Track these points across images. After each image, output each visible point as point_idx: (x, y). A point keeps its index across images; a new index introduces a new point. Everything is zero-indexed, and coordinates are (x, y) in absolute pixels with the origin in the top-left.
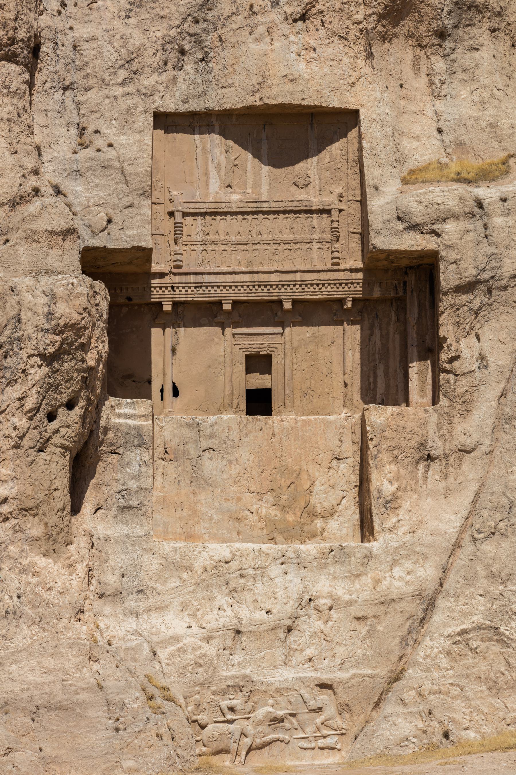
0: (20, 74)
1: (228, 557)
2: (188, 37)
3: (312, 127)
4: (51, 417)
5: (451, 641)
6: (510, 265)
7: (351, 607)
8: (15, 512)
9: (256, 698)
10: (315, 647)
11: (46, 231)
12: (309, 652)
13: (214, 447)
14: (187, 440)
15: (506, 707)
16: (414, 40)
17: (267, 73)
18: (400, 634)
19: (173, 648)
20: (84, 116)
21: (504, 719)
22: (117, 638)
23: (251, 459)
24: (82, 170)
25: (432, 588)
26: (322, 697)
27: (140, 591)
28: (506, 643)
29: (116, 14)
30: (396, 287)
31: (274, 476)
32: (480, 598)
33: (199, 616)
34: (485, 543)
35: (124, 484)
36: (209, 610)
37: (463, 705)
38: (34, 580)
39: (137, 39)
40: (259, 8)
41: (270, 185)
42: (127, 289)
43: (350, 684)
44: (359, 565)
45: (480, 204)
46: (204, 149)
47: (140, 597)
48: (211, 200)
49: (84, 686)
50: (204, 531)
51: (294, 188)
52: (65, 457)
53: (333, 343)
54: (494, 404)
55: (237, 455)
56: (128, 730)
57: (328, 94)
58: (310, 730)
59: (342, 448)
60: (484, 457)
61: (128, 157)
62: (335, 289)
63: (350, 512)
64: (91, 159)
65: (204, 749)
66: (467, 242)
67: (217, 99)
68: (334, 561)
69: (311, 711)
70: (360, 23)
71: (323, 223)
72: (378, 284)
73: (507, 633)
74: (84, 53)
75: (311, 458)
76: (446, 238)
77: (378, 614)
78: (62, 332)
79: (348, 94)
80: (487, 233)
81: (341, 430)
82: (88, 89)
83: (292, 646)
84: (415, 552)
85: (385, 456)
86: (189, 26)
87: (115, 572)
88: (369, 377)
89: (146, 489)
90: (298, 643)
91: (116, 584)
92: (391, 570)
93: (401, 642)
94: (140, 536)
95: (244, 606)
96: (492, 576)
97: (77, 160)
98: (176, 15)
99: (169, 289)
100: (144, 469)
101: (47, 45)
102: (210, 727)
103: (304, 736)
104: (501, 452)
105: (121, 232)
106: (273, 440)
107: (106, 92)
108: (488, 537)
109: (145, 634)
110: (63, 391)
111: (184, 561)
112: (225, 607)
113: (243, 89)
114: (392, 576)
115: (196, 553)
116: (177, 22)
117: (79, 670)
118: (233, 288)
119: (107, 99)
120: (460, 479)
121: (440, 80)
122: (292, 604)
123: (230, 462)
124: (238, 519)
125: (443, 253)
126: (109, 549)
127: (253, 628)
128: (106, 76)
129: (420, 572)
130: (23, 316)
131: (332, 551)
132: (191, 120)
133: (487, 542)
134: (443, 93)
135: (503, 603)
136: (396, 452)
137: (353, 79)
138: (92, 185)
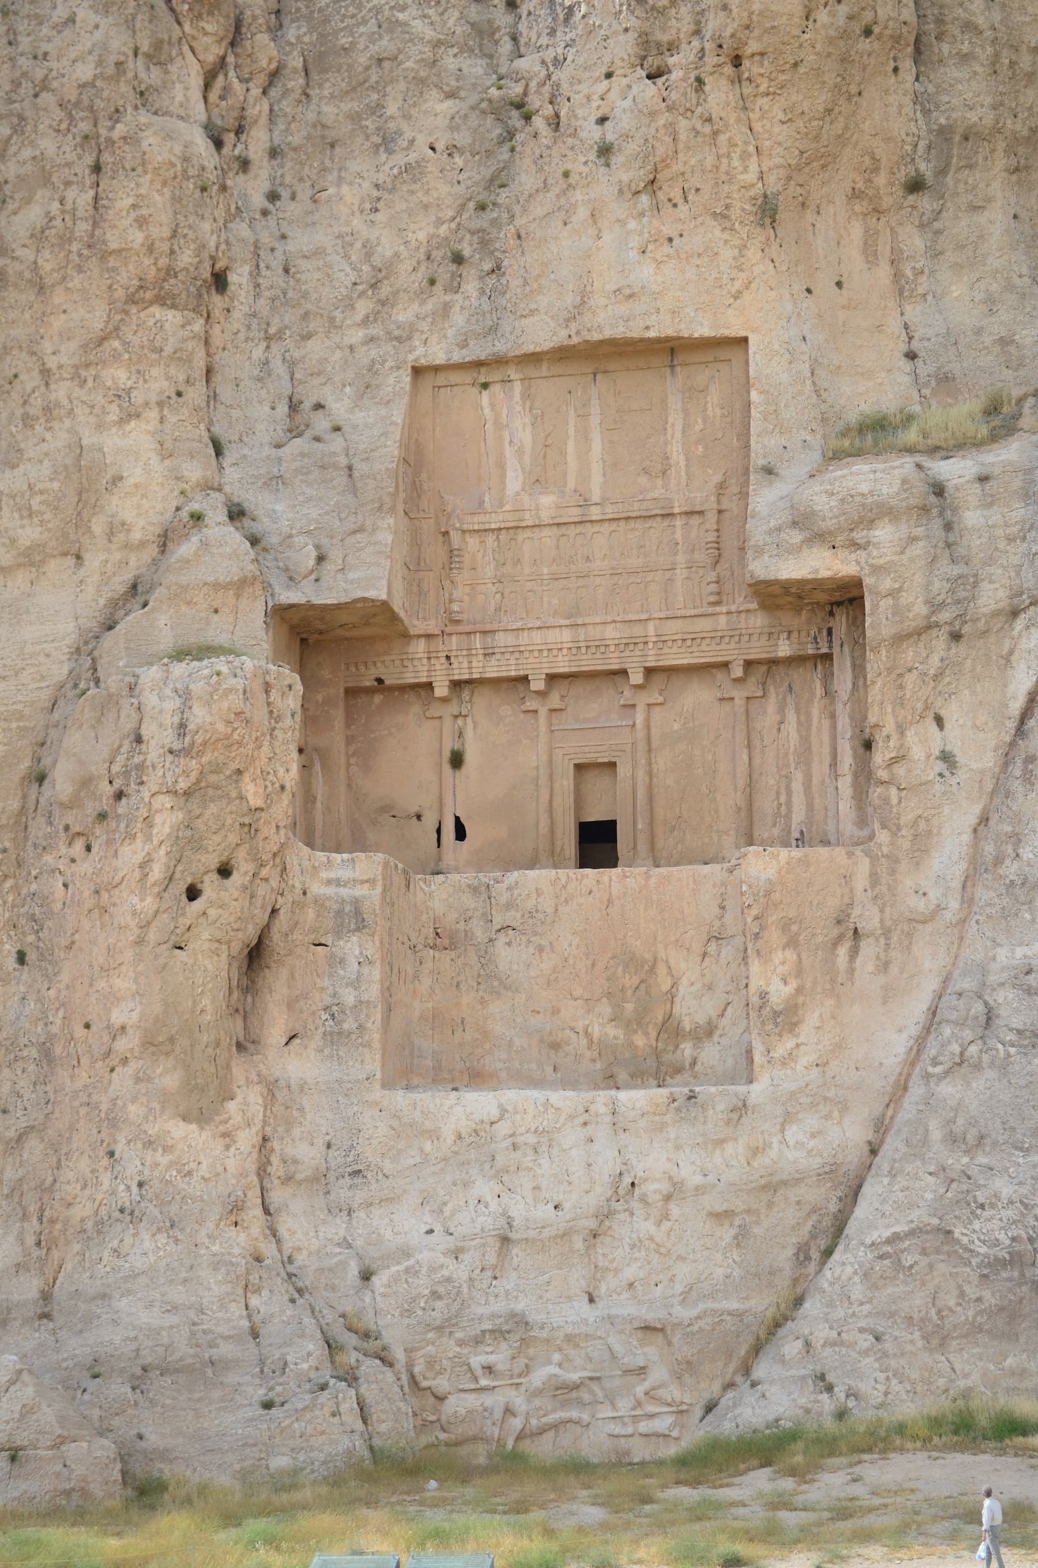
0: (183, 326)
1: (495, 1113)
2: (468, 236)
3: (673, 373)
5: (876, 1253)
6: (990, 593)
7: (706, 1197)
9: (531, 1351)
10: (639, 1264)
11: (205, 584)
12: (630, 1273)
13: (514, 924)
14: (470, 914)
15: (953, 1369)
16: (865, 203)
17: (589, 288)
18: (794, 1240)
19: (397, 1268)
20: (301, 382)
21: (946, 1391)
22: (305, 1253)
23: (574, 943)
24: (287, 475)
25: (856, 1160)
26: (646, 1349)
28: (962, 1258)
29: (355, 208)
30: (815, 638)
32: (930, 1178)
33: (447, 1214)
34: (944, 1082)
35: (335, 995)
36: (462, 1203)
37: (877, 1365)
38: (164, 1160)
40: (577, 177)
41: (604, 475)
42: (375, 663)
43: (696, 1328)
44: (721, 1123)
45: (939, 490)
46: (497, 422)
47: (356, 1181)
48: (508, 508)
49: (227, 1333)
50: (499, 1065)
51: (643, 480)
54: (967, 838)
56: (286, 1407)
57: (692, 314)
58: (624, 1406)
59: (724, 920)
60: (949, 931)
61: (362, 447)
62: (714, 647)
64: (302, 455)
65: (443, 1436)
66: (912, 560)
67: (513, 337)
69: (627, 1372)
70: (753, 185)
71: (693, 535)
72: (785, 635)
73: (965, 1240)
74: (303, 277)
75: (673, 938)
76: (875, 553)
77: (755, 1207)
78: (200, 753)
79: (730, 311)
80: (951, 539)
81: (723, 889)
82: (308, 337)
83: (601, 1264)
84: (826, 1099)
85: (774, 936)
86: (471, 219)
88: (778, 793)
89: (368, 1002)
90: (610, 1257)
92: (782, 1131)
93: (796, 1255)
94: (358, 1081)
95: (519, 1197)
96: (953, 1140)
97: (280, 460)
98: (449, 201)
99: (443, 660)
100: (365, 970)
101: (239, 271)
102: (452, 1400)
103: (615, 1414)
104: (977, 922)
105: (340, 576)
106: (610, 910)
107: (337, 339)
108: (947, 1073)
109: (359, 1243)
110: (211, 849)
111: (426, 1122)
112: (488, 1198)
113: (552, 318)
114: (784, 1141)
115: (445, 1108)
116: (451, 213)
117: (223, 1307)
118: (545, 653)
119: (338, 351)
121: (914, 268)
122: (601, 1191)
123: (541, 949)
124: (555, 1046)
125: (868, 581)
127: (532, 1234)
128: (338, 314)
129: (834, 1134)
130: (144, 732)
131: (674, 1100)
132: (475, 375)
134: (921, 290)
136: (795, 928)
137: (737, 285)
138: (301, 498)
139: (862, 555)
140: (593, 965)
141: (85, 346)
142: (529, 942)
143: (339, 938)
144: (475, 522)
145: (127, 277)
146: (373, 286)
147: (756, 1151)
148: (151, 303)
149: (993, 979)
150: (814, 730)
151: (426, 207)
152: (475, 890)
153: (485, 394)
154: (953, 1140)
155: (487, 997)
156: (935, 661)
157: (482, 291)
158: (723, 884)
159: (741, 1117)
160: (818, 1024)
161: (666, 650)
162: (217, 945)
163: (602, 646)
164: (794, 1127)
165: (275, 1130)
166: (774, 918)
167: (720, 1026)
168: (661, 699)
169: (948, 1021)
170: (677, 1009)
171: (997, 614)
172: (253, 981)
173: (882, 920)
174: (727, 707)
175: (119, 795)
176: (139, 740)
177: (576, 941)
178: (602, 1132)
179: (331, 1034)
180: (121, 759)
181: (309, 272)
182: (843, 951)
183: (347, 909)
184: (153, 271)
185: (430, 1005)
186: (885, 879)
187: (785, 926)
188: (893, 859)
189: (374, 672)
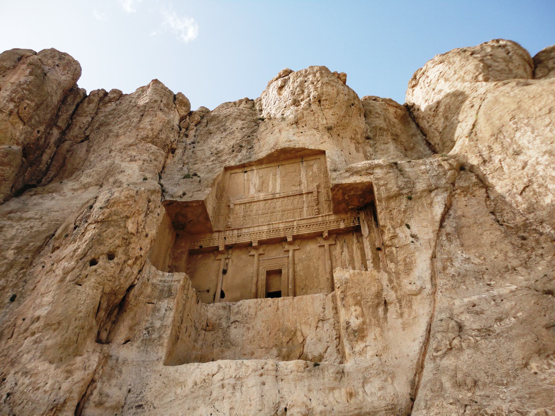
4: (93, 262)
8: (41, 328)
13: (239, 320)
25: (404, 403)
27: (140, 406)
31: (278, 335)
32: (451, 406)
39: (221, 147)
44: (331, 379)
51: (293, 188)
52: (97, 290)
53: (319, 258)
54: (428, 262)
55: (253, 324)
63: (333, 358)
68: (309, 375)
75: (303, 321)
81: (324, 302)
82: (196, 164)
84: (383, 371)
85: (350, 300)
87: (123, 388)
89: (166, 325)
91: (120, 398)
92: (363, 387)
94: (153, 361)
96: (458, 385)
100: (168, 313)
104: (441, 292)
108: (445, 354)
110: (106, 245)
111: (181, 378)
120: (413, 314)
123: (248, 329)
126: (124, 369)
129: (390, 389)
130: (94, 206)
131: (307, 367)
133: (446, 358)
135: (477, 407)
136: (359, 298)
139: (372, 176)
140: (270, 334)
141: (125, 146)
142: (244, 326)
143: (160, 301)
144: (238, 202)
145: (143, 134)
146: (216, 154)
147: (351, 395)
148: (149, 142)
149: (455, 312)
150: (354, 252)
151: (234, 139)
152: (224, 308)
153: (246, 174)
154: (458, 385)
155: (224, 349)
156: (403, 207)
157: (247, 152)
158: (324, 300)
159: (341, 377)
160: (374, 337)
161: (300, 229)
162: (98, 285)
163: (278, 230)
164: (369, 385)
165: (101, 377)
166: (350, 293)
167: (325, 356)
168: (298, 248)
169: (438, 332)
170: (305, 350)
171: (423, 191)
172: (118, 319)
173: (396, 296)
174: (322, 249)
175: (75, 228)
176: (91, 207)
177: (263, 324)
178: (269, 379)
179: (146, 340)
180: (81, 216)
181: (199, 154)
182: (381, 309)
183: (166, 289)
184: (151, 134)
185: (200, 352)
186: (395, 281)
187: (355, 296)
188: (398, 274)
189: (199, 244)
